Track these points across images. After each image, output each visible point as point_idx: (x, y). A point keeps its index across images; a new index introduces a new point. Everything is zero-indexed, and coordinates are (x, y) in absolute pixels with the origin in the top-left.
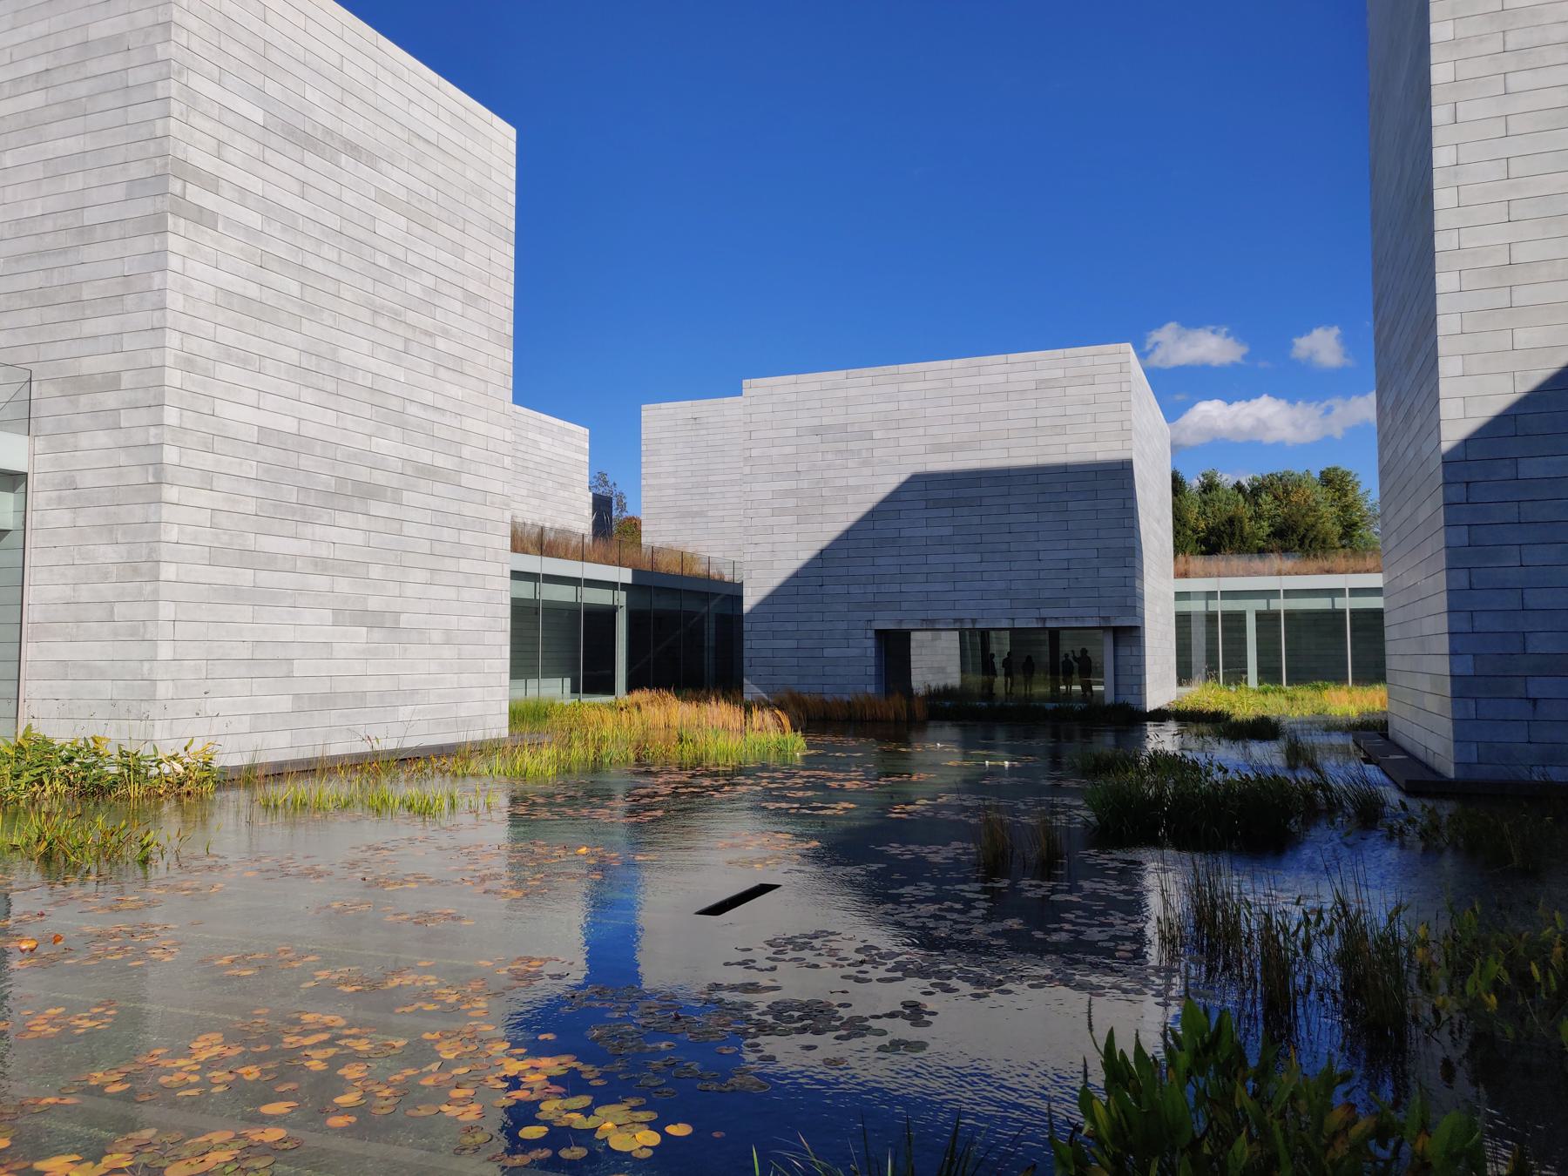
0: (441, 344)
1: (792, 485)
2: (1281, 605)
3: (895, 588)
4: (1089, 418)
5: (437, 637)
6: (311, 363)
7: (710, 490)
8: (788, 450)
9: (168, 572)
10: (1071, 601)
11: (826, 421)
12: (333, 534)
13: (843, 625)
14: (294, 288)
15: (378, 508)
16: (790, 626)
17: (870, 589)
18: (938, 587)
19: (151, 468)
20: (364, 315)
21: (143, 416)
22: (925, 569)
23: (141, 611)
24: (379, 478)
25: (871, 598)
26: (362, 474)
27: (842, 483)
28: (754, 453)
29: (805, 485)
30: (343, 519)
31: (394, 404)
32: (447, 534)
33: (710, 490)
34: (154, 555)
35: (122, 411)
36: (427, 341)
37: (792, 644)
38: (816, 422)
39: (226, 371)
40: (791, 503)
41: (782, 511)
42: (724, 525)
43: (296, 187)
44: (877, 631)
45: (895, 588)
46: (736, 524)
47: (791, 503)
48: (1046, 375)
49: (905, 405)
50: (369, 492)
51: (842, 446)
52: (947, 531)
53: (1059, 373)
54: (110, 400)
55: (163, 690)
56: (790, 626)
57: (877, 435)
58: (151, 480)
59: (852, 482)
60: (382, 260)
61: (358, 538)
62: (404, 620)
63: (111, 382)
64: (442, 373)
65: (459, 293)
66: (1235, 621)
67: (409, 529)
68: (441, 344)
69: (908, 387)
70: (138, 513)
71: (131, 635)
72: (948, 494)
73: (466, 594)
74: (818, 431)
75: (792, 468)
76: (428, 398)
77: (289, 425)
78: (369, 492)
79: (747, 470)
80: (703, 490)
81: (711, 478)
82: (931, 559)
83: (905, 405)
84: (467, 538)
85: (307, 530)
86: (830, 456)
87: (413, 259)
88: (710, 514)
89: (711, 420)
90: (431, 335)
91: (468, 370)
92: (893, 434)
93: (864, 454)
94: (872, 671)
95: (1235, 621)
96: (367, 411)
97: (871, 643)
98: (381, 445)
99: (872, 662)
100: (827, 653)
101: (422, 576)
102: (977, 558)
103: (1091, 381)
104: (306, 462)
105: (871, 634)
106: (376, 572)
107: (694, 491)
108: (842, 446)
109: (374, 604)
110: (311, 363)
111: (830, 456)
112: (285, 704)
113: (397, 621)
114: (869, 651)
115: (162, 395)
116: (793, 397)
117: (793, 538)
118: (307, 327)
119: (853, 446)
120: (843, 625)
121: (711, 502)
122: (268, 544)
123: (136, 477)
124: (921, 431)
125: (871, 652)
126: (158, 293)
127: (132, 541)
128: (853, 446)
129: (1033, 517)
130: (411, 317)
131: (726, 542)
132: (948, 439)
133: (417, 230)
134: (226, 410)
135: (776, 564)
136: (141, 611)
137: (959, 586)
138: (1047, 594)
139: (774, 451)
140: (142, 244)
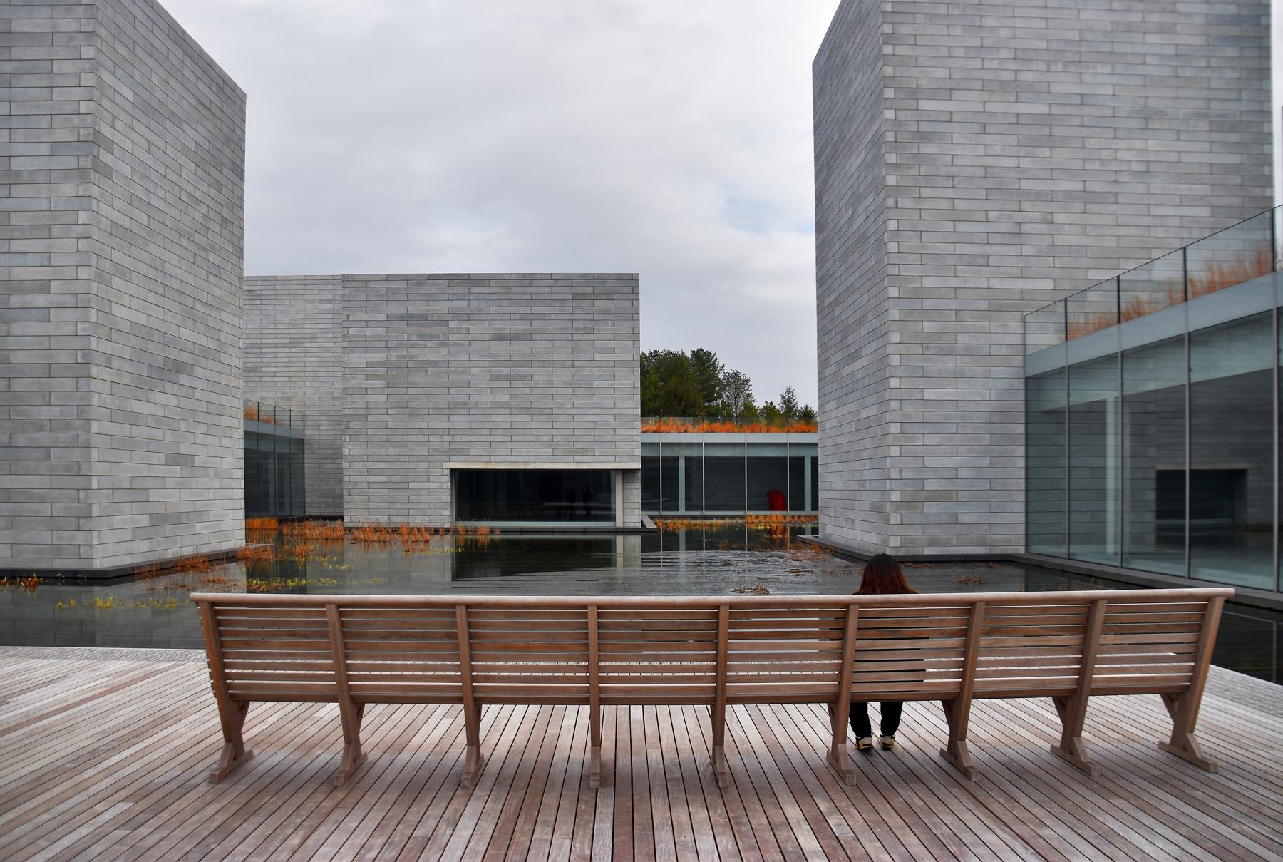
0: (211, 257)
1: (384, 357)
2: (704, 453)
3: (465, 439)
4: (610, 323)
5: (211, 473)
6: (152, 274)
7: (263, 350)
8: (380, 330)
9: (95, 427)
10: (597, 451)
11: (411, 310)
12: (162, 398)
13: (425, 465)
14: (144, 219)
15: (184, 379)
16: (382, 466)
17: (446, 439)
18: (499, 439)
19: (79, 352)
20: (175, 237)
21: (72, 315)
22: (489, 425)
23: (76, 454)
24: (184, 357)
25: (446, 445)
26: (174, 354)
27: (425, 358)
28: (351, 331)
29: (394, 358)
30: (169, 387)
31: (189, 302)
32: (214, 398)
33: (263, 350)
34: (85, 415)
35: (51, 310)
36: (203, 254)
37: (384, 478)
38: (403, 311)
39: (117, 283)
40: (382, 371)
41: (375, 377)
42: (275, 379)
43: (145, 145)
44: (452, 471)
45: (465, 439)
46: (287, 379)
47: (382, 371)
48: (580, 290)
49: (475, 304)
50: (179, 368)
51: (424, 330)
52: (507, 398)
53: (589, 290)
54: (40, 300)
55: (96, 510)
56: (382, 466)
57: (452, 324)
58: (79, 361)
59: (432, 358)
60: (184, 197)
61: (173, 401)
62: (198, 461)
63: (44, 288)
64: (212, 278)
65: (218, 218)
66: (671, 463)
67: (198, 394)
68: (211, 257)
69: (475, 290)
70: (69, 384)
71: (67, 471)
72: (506, 371)
73: (226, 442)
74: (403, 317)
75: (382, 344)
76: (204, 297)
77: (141, 319)
78: (179, 368)
79: (345, 344)
80: (256, 351)
81: (264, 341)
82: (493, 418)
83: (475, 304)
84: (224, 400)
85: (153, 396)
86: (414, 338)
87: (198, 195)
88: (263, 370)
89: (264, 293)
90: (205, 250)
91: (223, 276)
92: (465, 324)
93: (442, 337)
94: (448, 499)
95: (671, 463)
96: (177, 308)
97: (448, 478)
98: (185, 333)
99: (448, 493)
100: (412, 485)
101: (203, 429)
102: (528, 418)
103: (612, 298)
104: (152, 347)
105: (447, 472)
106: (183, 426)
107: (248, 351)
108: (424, 330)
109: (183, 449)
110: (152, 274)
111: (414, 338)
112: (144, 520)
113: (193, 462)
114: (445, 484)
115: (89, 300)
116: (384, 291)
117: (384, 398)
118: (152, 248)
119: (432, 330)
120: (425, 465)
121: (264, 360)
122: (138, 407)
123: (65, 358)
124: (486, 324)
125: (447, 485)
126: (82, 226)
127: (63, 404)
128: (432, 330)
129: (570, 391)
130: (197, 237)
131: (278, 394)
132: (507, 331)
133: (200, 172)
134: (118, 310)
135: (370, 418)
136: (76, 454)
137: (515, 438)
138: (579, 446)
139: (368, 331)
140: (68, 190)
